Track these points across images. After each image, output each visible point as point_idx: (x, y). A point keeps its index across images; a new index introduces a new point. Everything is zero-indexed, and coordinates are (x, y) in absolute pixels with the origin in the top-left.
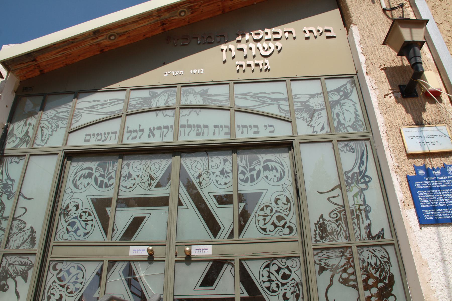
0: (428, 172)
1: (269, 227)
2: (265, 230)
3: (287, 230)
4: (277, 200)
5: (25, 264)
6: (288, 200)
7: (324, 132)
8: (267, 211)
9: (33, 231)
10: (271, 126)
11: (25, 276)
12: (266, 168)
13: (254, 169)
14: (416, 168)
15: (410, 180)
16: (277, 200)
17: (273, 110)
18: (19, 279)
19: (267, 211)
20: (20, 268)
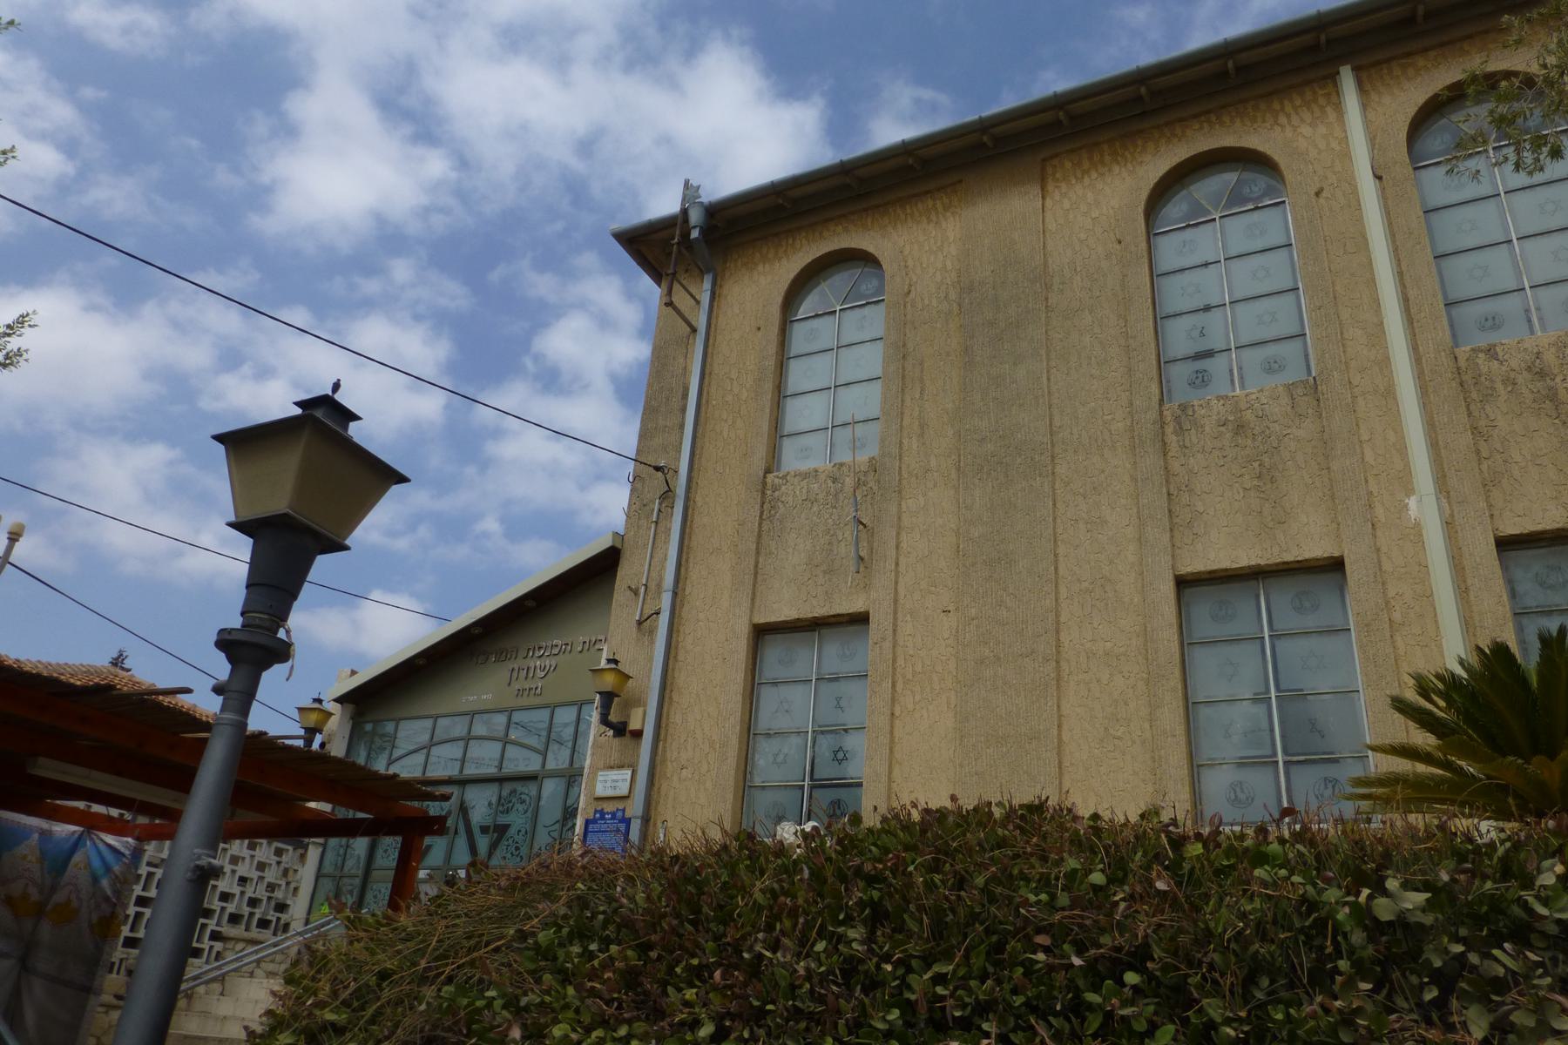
0: (602, 813)
1: (509, 856)
2: (505, 858)
3: (519, 859)
4: (519, 831)
5: (351, 885)
6: (526, 833)
7: (564, 766)
8: (510, 841)
9: (359, 857)
10: (529, 759)
11: (351, 893)
13: (510, 802)
14: (596, 811)
15: (587, 822)
16: (519, 831)
17: (533, 741)
18: (349, 896)
19: (510, 841)
20: (350, 888)
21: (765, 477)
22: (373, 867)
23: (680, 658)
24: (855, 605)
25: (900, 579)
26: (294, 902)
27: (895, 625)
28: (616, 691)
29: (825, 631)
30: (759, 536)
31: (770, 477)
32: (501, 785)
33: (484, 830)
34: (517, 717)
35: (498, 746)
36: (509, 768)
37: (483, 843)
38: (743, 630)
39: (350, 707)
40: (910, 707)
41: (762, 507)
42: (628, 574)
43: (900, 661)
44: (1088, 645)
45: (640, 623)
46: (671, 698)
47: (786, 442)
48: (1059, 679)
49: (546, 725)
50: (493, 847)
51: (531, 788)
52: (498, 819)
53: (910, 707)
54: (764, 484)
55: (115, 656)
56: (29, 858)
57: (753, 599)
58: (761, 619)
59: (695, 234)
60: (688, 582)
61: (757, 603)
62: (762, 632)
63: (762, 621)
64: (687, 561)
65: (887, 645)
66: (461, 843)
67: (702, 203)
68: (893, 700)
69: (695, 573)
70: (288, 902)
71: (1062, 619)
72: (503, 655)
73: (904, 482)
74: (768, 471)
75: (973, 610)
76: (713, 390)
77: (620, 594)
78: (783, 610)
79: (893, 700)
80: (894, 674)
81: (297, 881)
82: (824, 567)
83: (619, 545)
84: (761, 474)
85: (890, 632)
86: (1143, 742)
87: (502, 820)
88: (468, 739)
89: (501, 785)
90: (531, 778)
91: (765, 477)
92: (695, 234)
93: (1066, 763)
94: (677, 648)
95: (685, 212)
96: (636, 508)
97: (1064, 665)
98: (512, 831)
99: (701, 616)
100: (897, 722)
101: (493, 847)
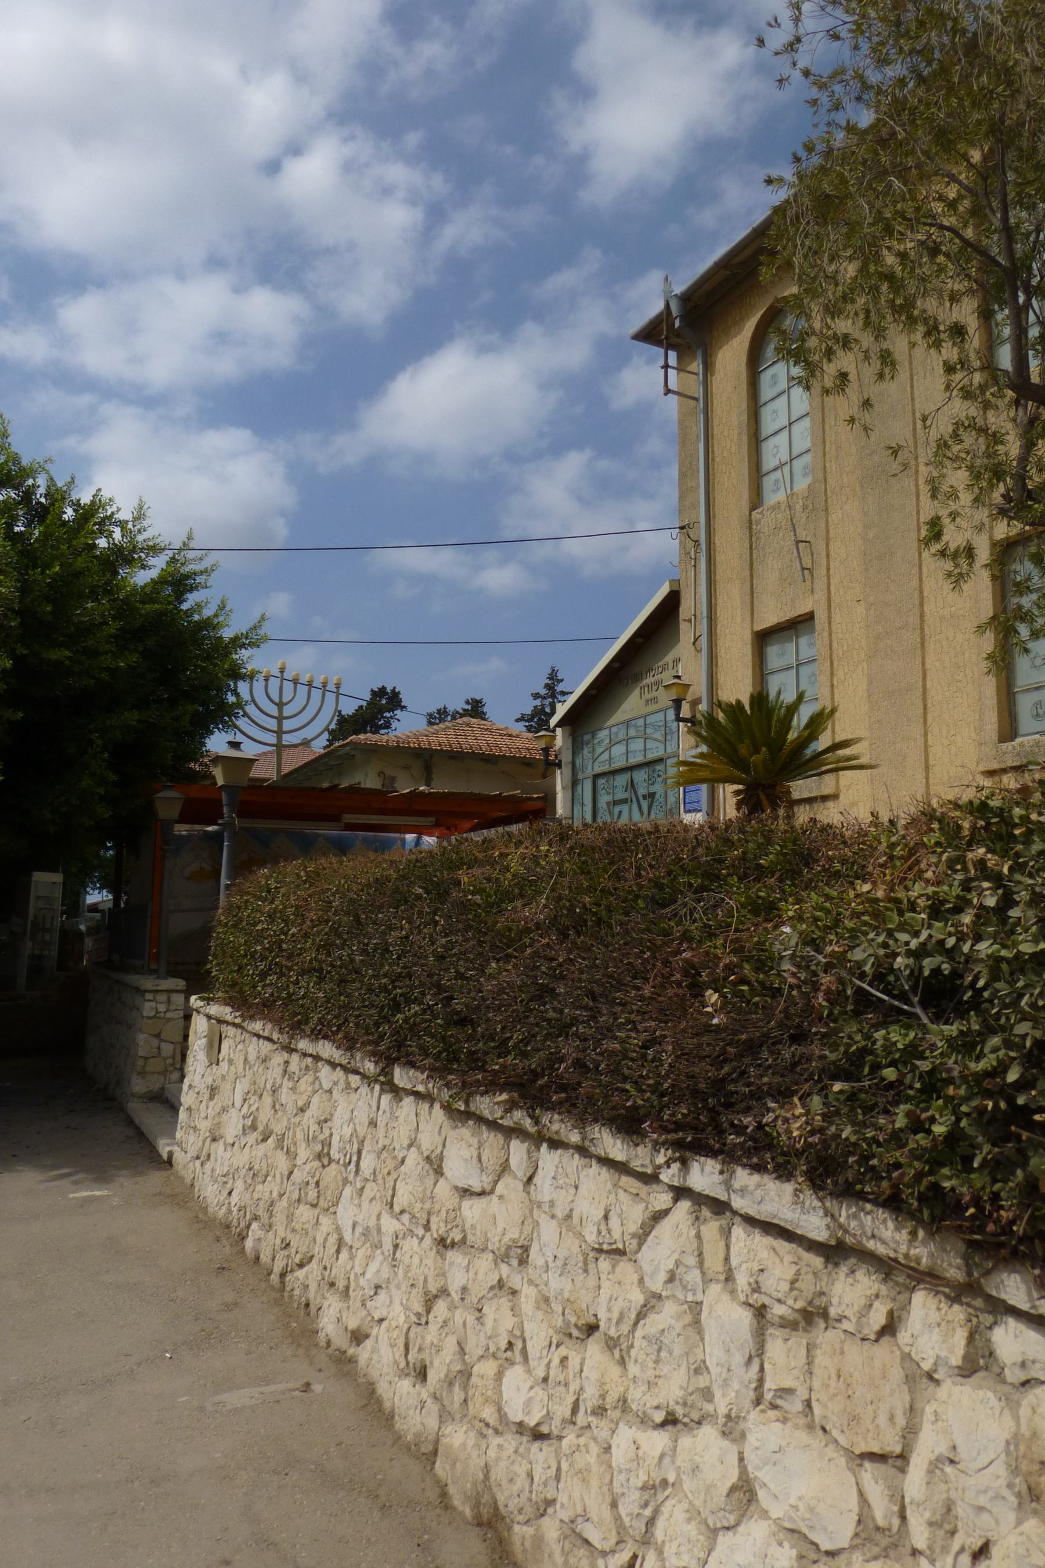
12: (659, 776)
21: (750, 515)
23: (720, 664)
24: (802, 609)
25: (832, 581)
27: (830, 617)
28: (681, 697)
29: (799, 627)
30: (751, 564)
31: (754, 513)
33: (644, 797)
34: (649, 720)
35: (642, 740)
36: (651, 756)
37: (645, 805)
38: (748, 637)
39: (568, 728)
40: (842, 678)
41: (751, 540)
42: (686, 609)
43: (835, 645)
44: (941, 612)
45: (694, 643)
47: (765, 480)
48: (923, 644)
49: (662, 723)
50: (650, 807)
51: (659, 767)
53: (842, 678)
54: (750, 521)
55: (550, 672)
57: (752, 614)
58: (758, 627)
59: (677, 323)
61: (756, 616)
62: (763, 638)
63: (759, 629)
65: (826, 634)
66: (635, 806)
67: (676, 295)
68: (832, 674)
69: (721, 600)
71: (925, 594)
72: (638, 678)
73: (829, 501)
74: (753, 508)
75: (872, 598)
76: (716, 449)
77: (683, 626)
78: (769, 618)
79: (832, 674)
80: (831, 655)
82: (789, 580)
83: (676, 588)
84: (747, 514)
85: (827, 625)
86: (973, 682)
87: (652, 789)
88: (627, 740)
90: (660, 760)
91: (750, 515)
92: (677, 323)
93: (929, 705)
95: (667, 306)
96: (688, 557)
97: (926, 630)
98: (657, 796)
99: (727, 631)
100: (836, 690)
101: (650, 807)
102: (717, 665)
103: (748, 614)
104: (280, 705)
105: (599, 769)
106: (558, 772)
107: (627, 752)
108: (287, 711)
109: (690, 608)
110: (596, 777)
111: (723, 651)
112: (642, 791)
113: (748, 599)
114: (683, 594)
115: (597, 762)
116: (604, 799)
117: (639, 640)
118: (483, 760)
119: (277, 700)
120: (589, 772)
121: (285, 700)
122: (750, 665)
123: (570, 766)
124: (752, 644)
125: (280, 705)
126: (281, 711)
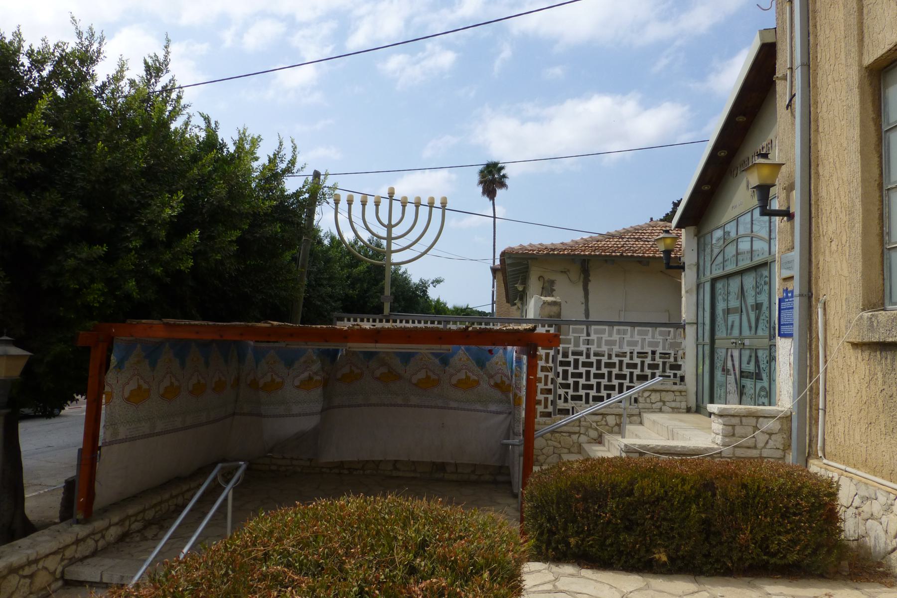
15: (780, 300)
22: (716, 337)
26: (684, 362)
28: (769, 182)
32: (756, 271)
35: (749, 239)
39: (692, 229)
46: (817, 173)
52: (758, 299)
56: (499, 363)
60: (818, 47)
63: (871, 60)
64: (815, 26)
70: (679, 363)
81: (683, 349)
83: (770, 40)
89: (756, 271)
94: (817, 121)
102: (817, 130)
103: (854, 43)
104: (389, 227)
105: (718, 272)
106: (683, 274)
107: (737, 254)
108: (396, 232)
109: (786, 61)
110: (714, 281)
111: (824, 109)
112: (750, 301)
113: (853, 20)
114: (779, 46)
115: (714, 265)
116: (721, 306)
117: (741, 119)
118: (640, 262)
119: (386, 223)
120: (708, 276)
121: (393, 223)
122: (857, 121)
123: (695, 269)
124: (861, 87)
125: (389, 227)
126: (389, 232)
